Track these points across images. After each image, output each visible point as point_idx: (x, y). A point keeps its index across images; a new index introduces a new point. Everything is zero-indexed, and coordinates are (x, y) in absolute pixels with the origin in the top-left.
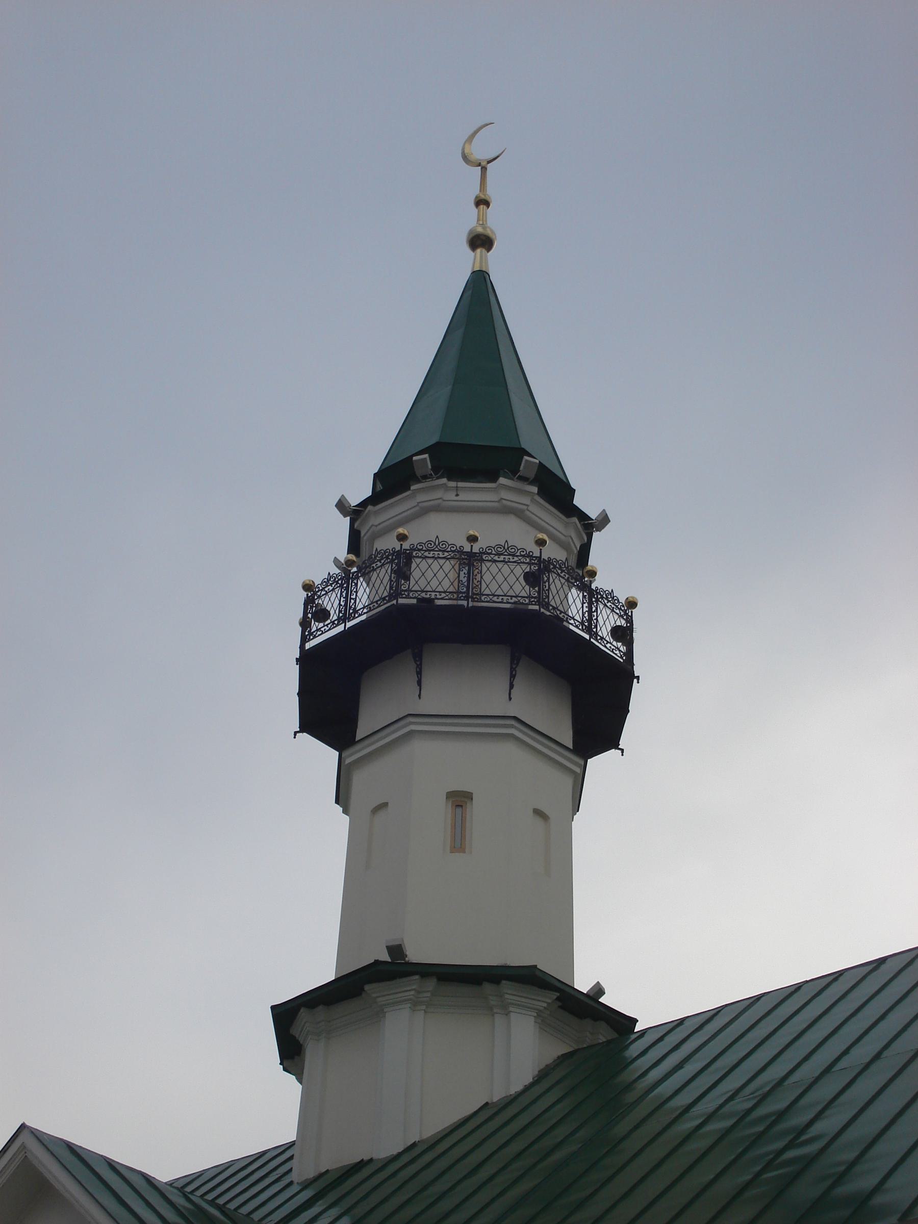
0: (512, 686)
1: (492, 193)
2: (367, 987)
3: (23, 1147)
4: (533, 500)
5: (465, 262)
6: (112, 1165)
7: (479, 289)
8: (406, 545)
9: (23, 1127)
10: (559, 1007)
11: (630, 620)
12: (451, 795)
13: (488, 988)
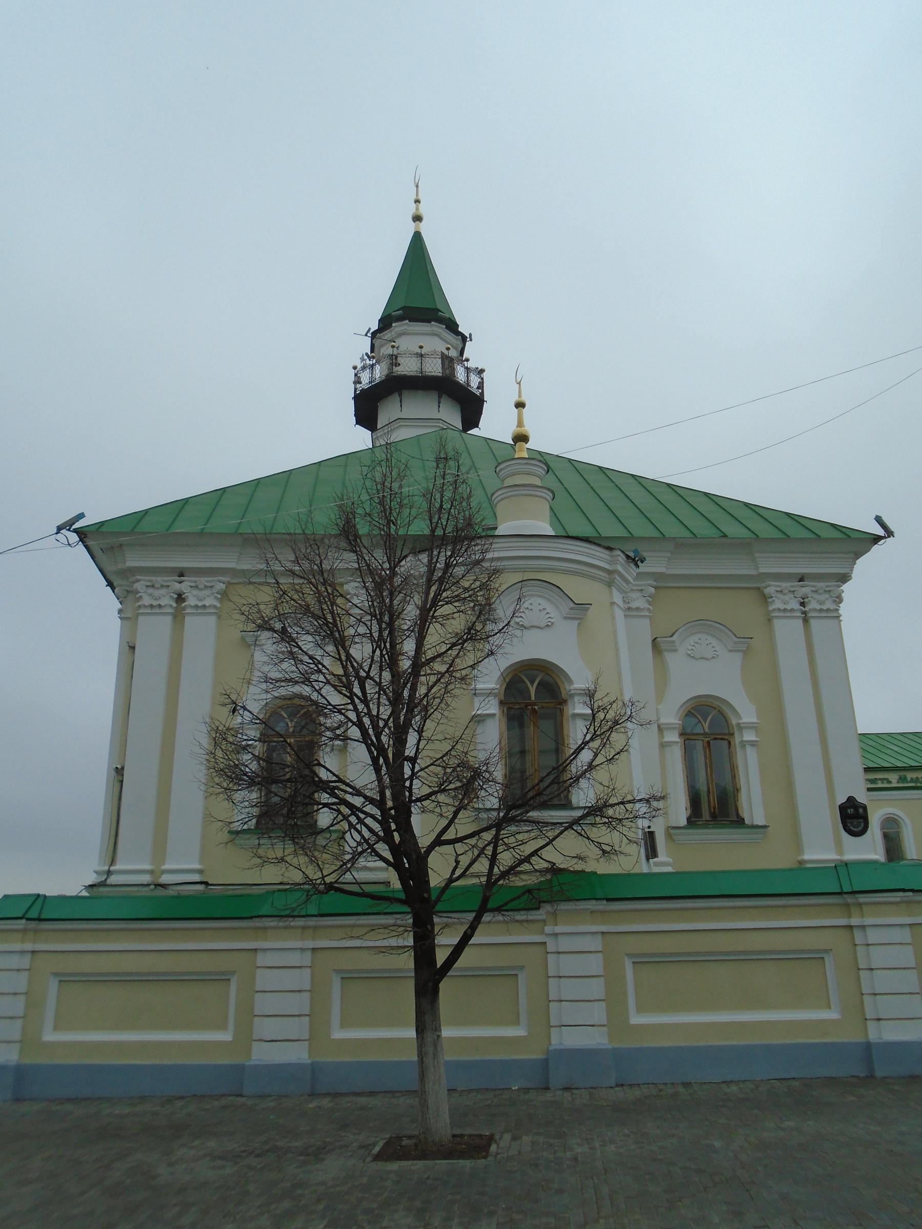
1: (421, 197)
5: (411, 228)
7: (417, 239)
11: (482, 379)
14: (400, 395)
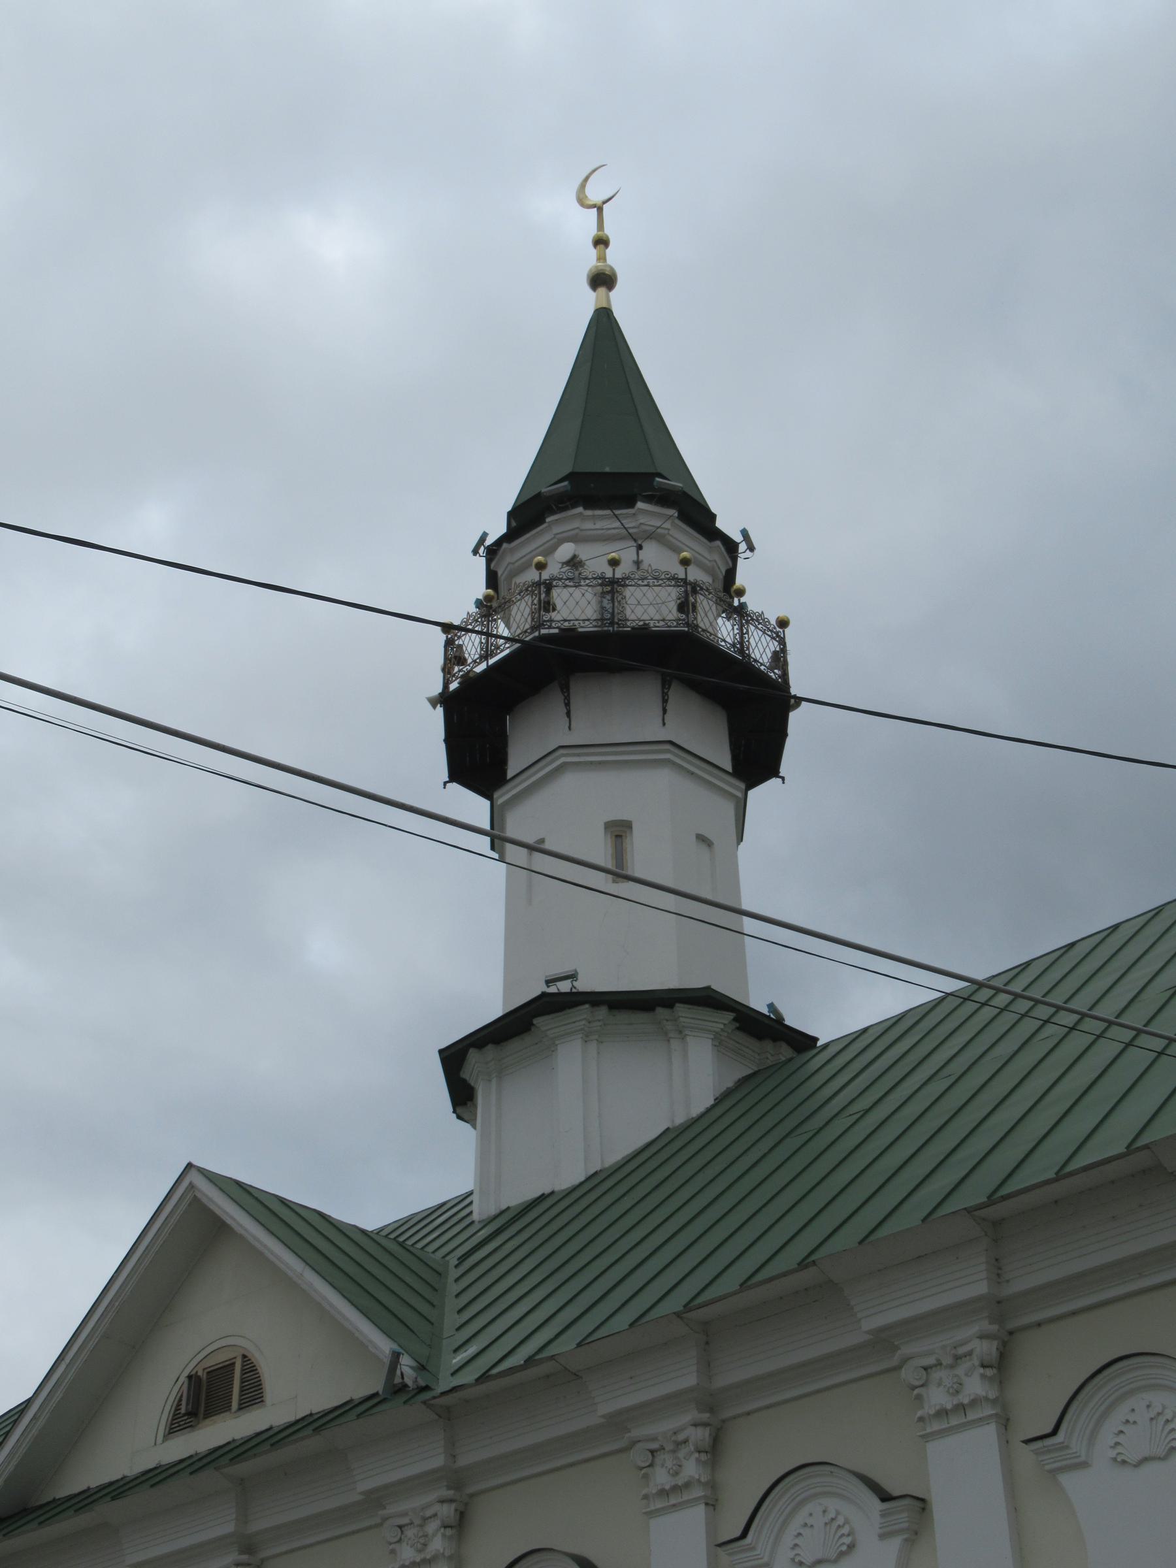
0: (665, 711)
1: (608, 231)
2: (535, 1021)
3: (192, 1186)
4: (673, 524)
5: (588, 301)
6: (283, 1201)
8: (546, 575)
9: (190, 1166)
10: (738, 1028)
11: (782, 642)
13: (660, 1010)
14: (565, 689)
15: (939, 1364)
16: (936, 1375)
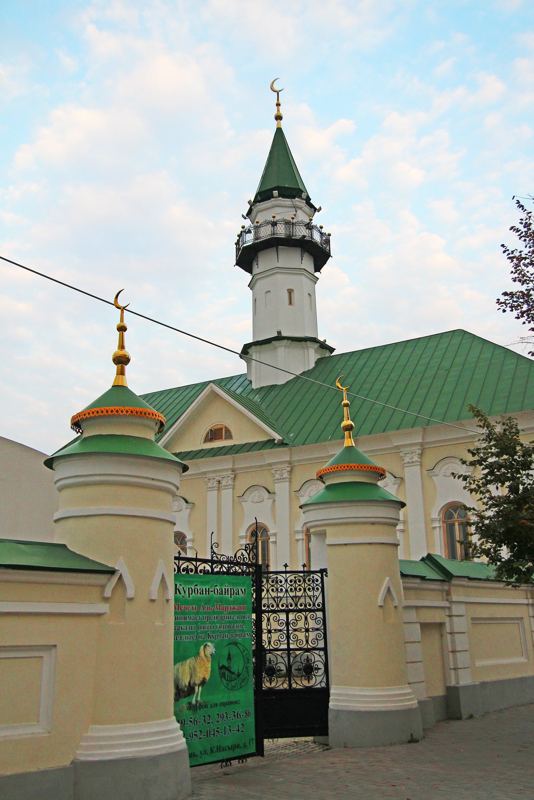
0: (302, 260)
5: (274, 125)
7: (279, 133)
8: (275, 220)
12: (288, 290)
13: (303, 342)
15: (408, 453)
16: (407, 455)
